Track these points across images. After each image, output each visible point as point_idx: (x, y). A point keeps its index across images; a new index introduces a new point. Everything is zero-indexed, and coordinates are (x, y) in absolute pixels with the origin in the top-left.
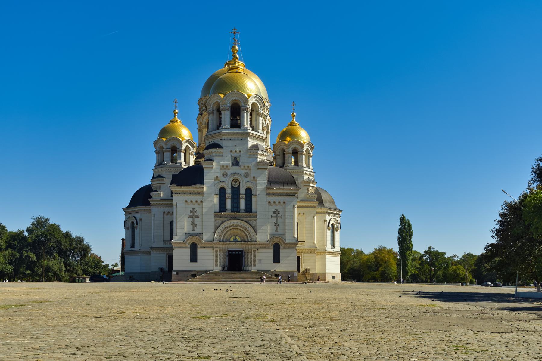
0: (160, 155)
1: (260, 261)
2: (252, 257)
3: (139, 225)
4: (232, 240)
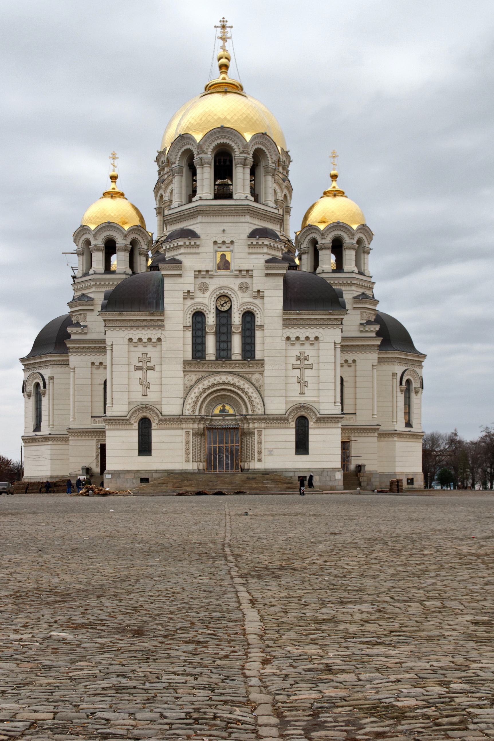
0: (85, 256)
3: (49, 390)
4: (217, 411)
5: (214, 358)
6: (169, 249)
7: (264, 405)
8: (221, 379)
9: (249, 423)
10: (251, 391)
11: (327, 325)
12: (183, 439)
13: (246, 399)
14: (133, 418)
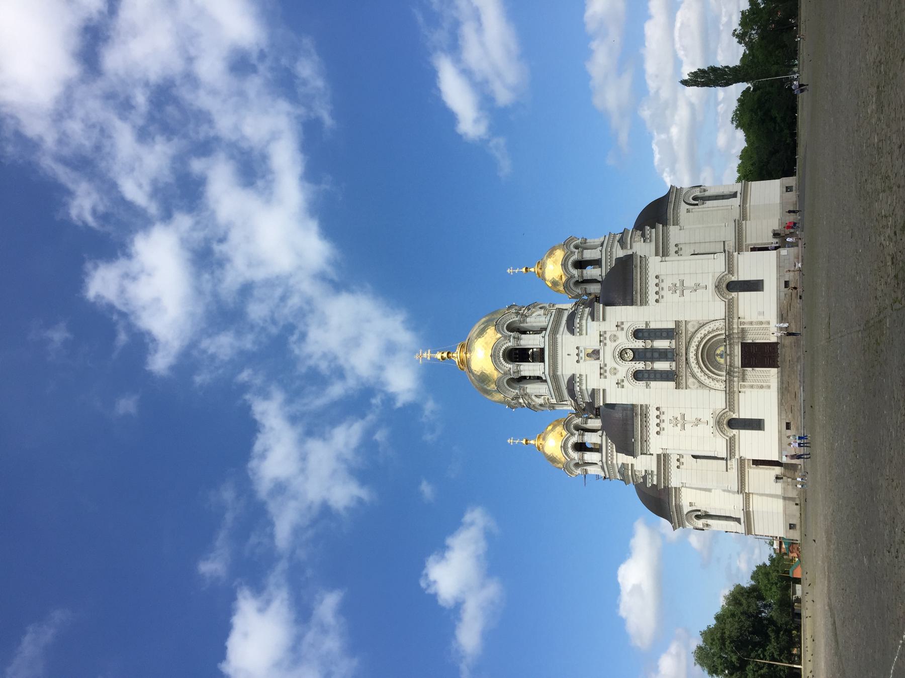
1: (760, 313)
2: (753, 326)
4: (722, 361)
5: (674, 364)
6: (582, 399)
7: (716, 320)
8: (692, 357)
9: (733, 333)
10: (703, 332)
11: (646, 269)
12: (748, 390)
13: (711, 335)
14: (728, 434)
